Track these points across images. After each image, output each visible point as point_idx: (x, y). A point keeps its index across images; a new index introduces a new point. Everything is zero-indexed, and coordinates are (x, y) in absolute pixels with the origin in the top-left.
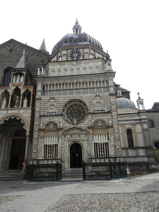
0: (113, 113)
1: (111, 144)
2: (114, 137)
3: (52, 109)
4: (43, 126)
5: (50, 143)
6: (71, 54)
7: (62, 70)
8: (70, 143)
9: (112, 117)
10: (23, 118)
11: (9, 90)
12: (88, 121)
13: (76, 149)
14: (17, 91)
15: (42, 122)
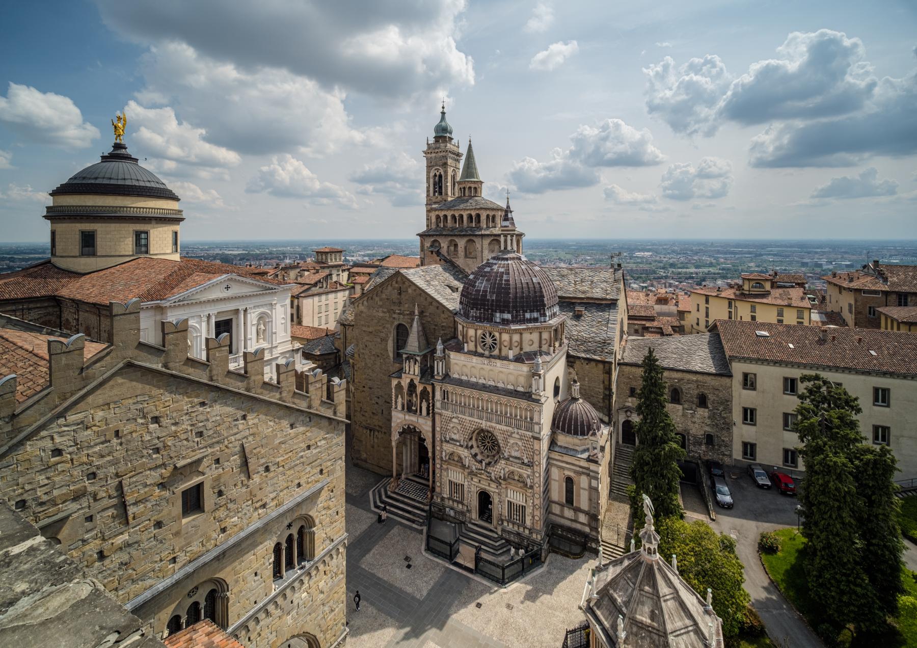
0: (535, 467)
1: (528, 511)
2: (533, 503)
3: (455, 434)
4: (446, 456)
5: (456, 481)
6: (482, 338)
7: (469, 367)
8: (478, 489)
9: (534, 473)
10: (423, 432)
11: (403, 384)
12: (501, 468)
13: (485, 499)
14: (412, 386)
15: (445, 448)
